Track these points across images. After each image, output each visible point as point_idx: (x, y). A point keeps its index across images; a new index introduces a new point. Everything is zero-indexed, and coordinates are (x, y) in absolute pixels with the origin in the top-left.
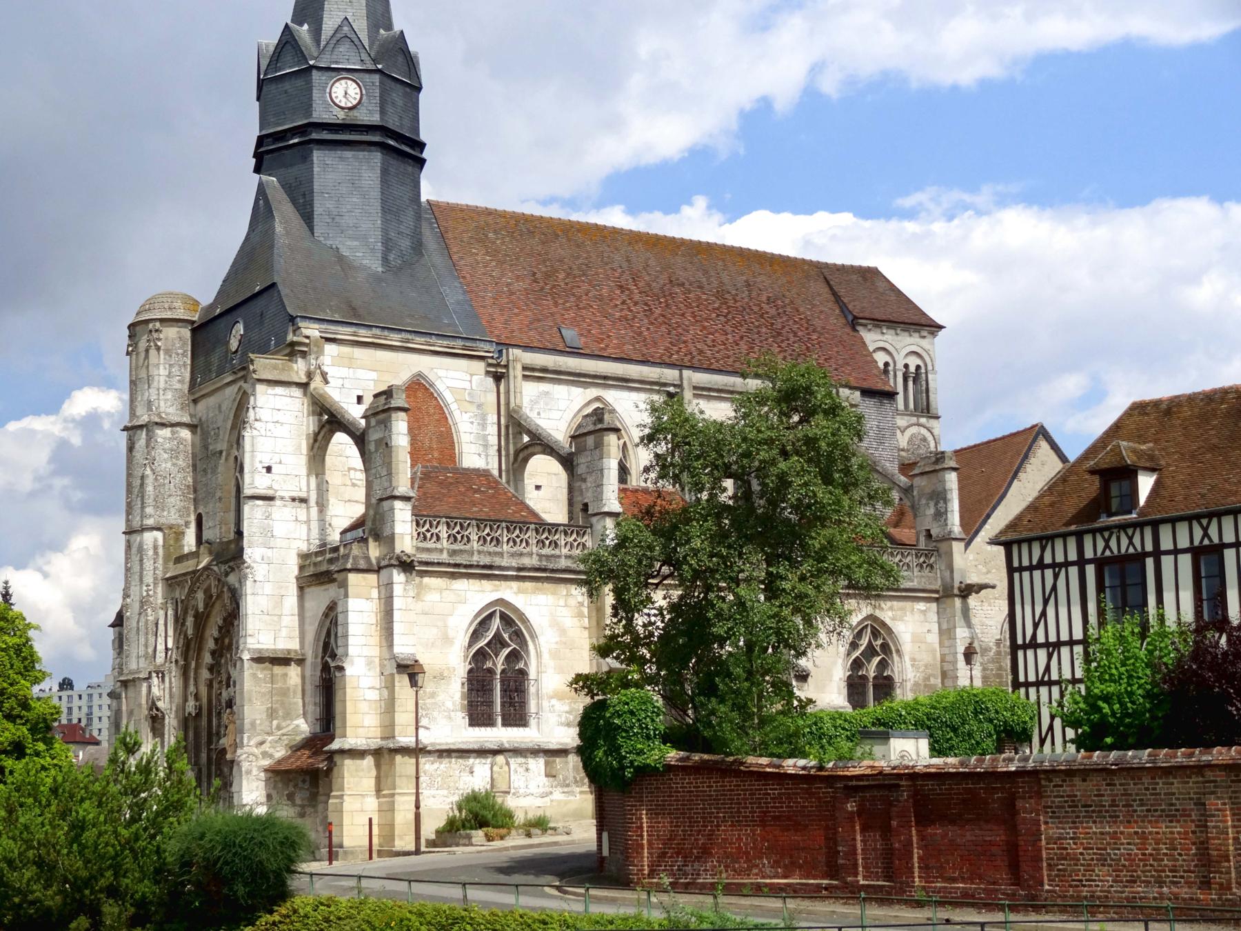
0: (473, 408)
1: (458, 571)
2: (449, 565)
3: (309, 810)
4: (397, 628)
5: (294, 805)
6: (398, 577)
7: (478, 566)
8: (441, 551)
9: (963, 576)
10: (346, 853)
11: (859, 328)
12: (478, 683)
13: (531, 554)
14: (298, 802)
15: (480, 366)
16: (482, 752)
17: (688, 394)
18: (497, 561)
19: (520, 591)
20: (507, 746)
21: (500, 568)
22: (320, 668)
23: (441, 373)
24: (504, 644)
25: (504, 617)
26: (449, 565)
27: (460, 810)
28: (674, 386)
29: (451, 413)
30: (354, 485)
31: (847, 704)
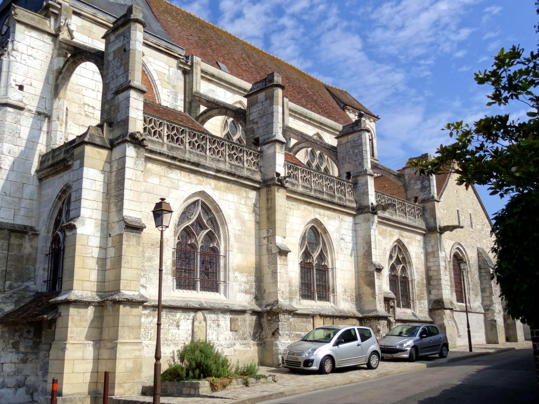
1: (174, 163)
2: (168, 156)
3: (31, 357)
4: (127, 194)
5: (18, 352)
6: (131, 151)
7: (189, 162)
8: (163, 144)
9: (440, 223)
10: (64, 401)
11: (346, 110)
12: (184, 254)
14: (22, 349)
15: (174, 62)
16: (186, 309)
18: (202, 161)
19: (216, 188)
20: (205, 305)
21: (204, 167)
22: (50, 240)
23: (151, 59)
26: (168, 156)
27: (182, 359)
29: (155, 86)
30: (87, 116)
31: (390, 291)
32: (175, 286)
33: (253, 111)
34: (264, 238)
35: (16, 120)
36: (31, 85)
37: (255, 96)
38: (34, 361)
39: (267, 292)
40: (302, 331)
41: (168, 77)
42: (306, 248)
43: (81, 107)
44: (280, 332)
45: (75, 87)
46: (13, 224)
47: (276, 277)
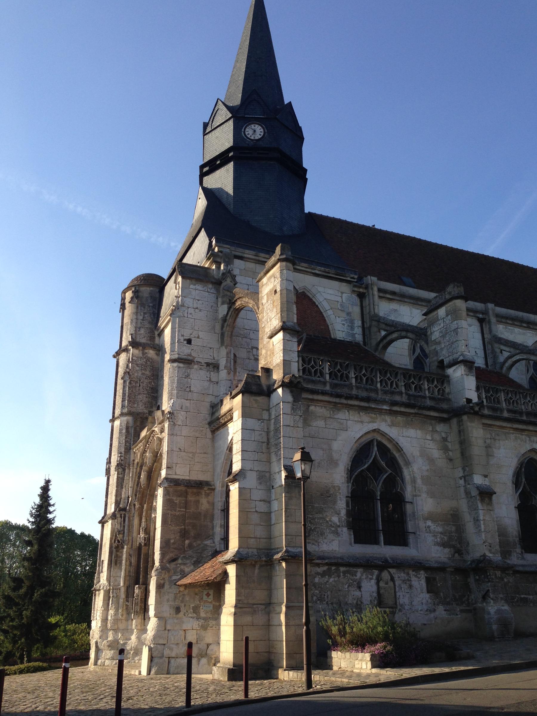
0: (344, 315)
7: (357, 398)
8: (325, 383)
13: (401, 393)
14: (203, 615)
17: (493, 320)
18: (373, 395)
19: (393, 425)
24: (381, 471)
25: (380, 445)
26: (331, 395)
28: (483, 314)
32: (353, 540)
33: (435, 329)
34: (461, 478)
35: (186, 374)
36: (198, 337)
37: (435, 313)
38: (214, 627)
39: (471, 545)
40: (529, 594)
41: (341, 305)
42: (524, 487)
43: (250, 352)
44: (491, 595)
45: (242, 332)
46: (189, 480)
47: (479, 526)
